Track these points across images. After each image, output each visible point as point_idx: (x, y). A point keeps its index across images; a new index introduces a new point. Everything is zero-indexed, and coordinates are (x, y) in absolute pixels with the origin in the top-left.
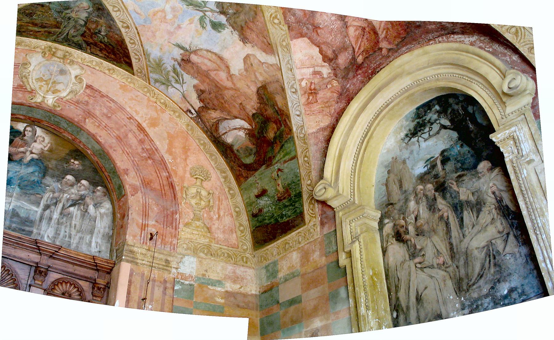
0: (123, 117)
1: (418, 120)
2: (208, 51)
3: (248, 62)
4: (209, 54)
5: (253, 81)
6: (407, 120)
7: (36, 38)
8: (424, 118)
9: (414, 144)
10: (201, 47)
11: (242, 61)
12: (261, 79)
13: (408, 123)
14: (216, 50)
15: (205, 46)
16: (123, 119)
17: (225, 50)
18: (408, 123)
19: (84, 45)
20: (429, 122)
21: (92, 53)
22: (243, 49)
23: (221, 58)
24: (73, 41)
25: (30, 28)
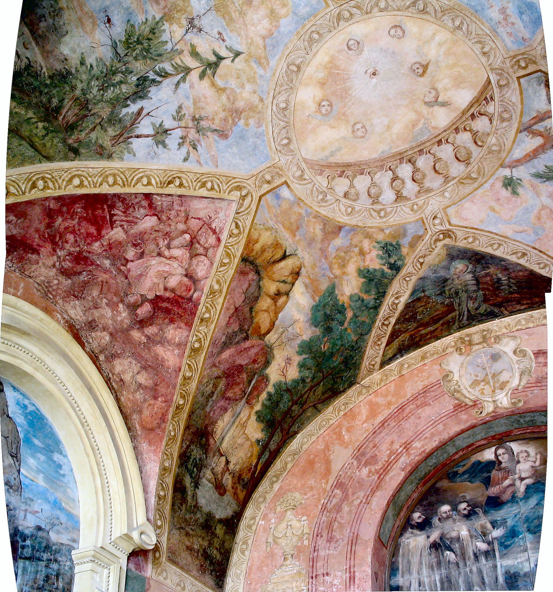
7: (438, 338)
19: (496, 310)
21: (512, 313)
24: (480, 313)
25: (423, 332)
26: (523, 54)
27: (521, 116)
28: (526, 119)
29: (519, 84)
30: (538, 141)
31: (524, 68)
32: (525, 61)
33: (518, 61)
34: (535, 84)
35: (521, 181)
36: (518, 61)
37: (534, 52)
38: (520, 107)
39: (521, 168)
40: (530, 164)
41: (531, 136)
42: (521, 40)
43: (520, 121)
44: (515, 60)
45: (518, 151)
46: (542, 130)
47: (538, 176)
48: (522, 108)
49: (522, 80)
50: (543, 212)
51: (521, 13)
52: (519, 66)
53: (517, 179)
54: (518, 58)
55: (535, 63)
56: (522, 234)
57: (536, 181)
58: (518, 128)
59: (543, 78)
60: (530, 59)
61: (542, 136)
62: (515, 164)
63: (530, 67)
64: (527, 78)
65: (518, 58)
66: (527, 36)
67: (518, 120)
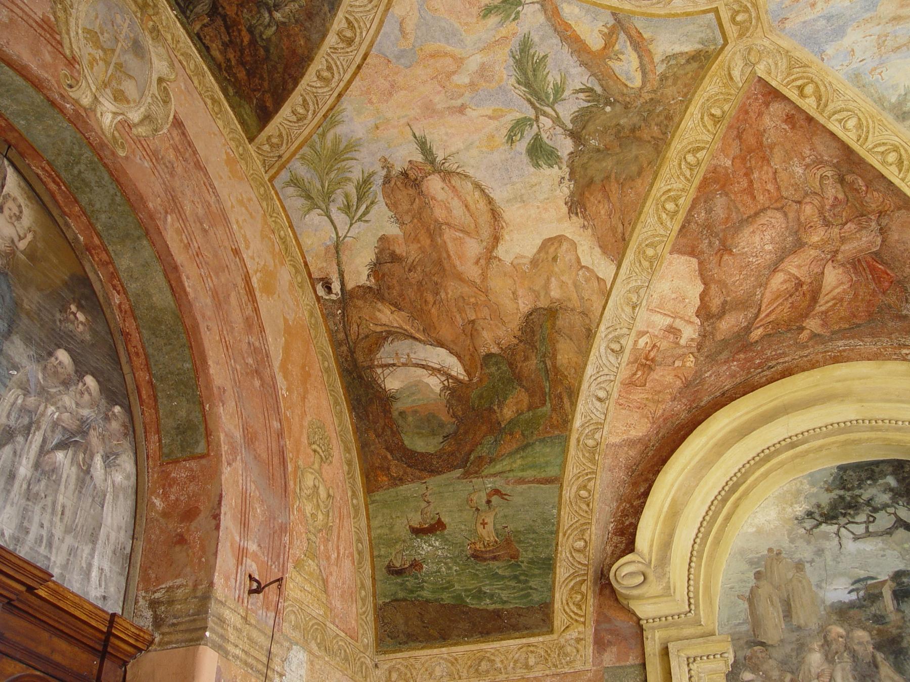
0: (226, 243)
1: (842, 492)
2: (478, 186)
3: (552, 250)
4: (477, 194)
5: (534, 291)
6: (813, 484)
8: (857, 492)
9: (826, 536)
10: (471, 172)
11: (539, 242)
12: (555, 293)
13: (815, 490)
14: (499, 195)
15: (479, 175)
16: (225, 247)
17: (519, 205)
18: (815, 490)
20: (868, 503)
22: (560, 220)
23: (495, 215)
26: (758, 18)
27: (643, 14)
28: (639, 23)
29: (705, 12)
30: (595, 42)
31: (733, 20)
32: (744, 22)
33: (746, 10)
34: (703, 35)
35: (514, 20)
36: (746, 10)
37: (761, 34)
38: (662, 12)
39: (541, 18)
40: (551, 31)
41: (606, 30)
42: (782, 16)
43: (634, 13)
44: (749, 5)
45: (577, 10)
46: (617, 47)
47: (525, 45)
48: (659, 16)
49: (712, 15)
50: (448, 61)
51: (829, 18)
52: (738, 12)
53: (518, 13)
54: (752, 10)
55: (741, 35)
56: (397, 32)
57: (514, 44)
58: (621, 10)
59: (712, 47)
60: (747, 29)
61: (605, 48)
62: (549, 7)
63: (734, 28)
64: (715, 22)
65: (752, 10)
66: (788, 25)
67: (638, 10)
